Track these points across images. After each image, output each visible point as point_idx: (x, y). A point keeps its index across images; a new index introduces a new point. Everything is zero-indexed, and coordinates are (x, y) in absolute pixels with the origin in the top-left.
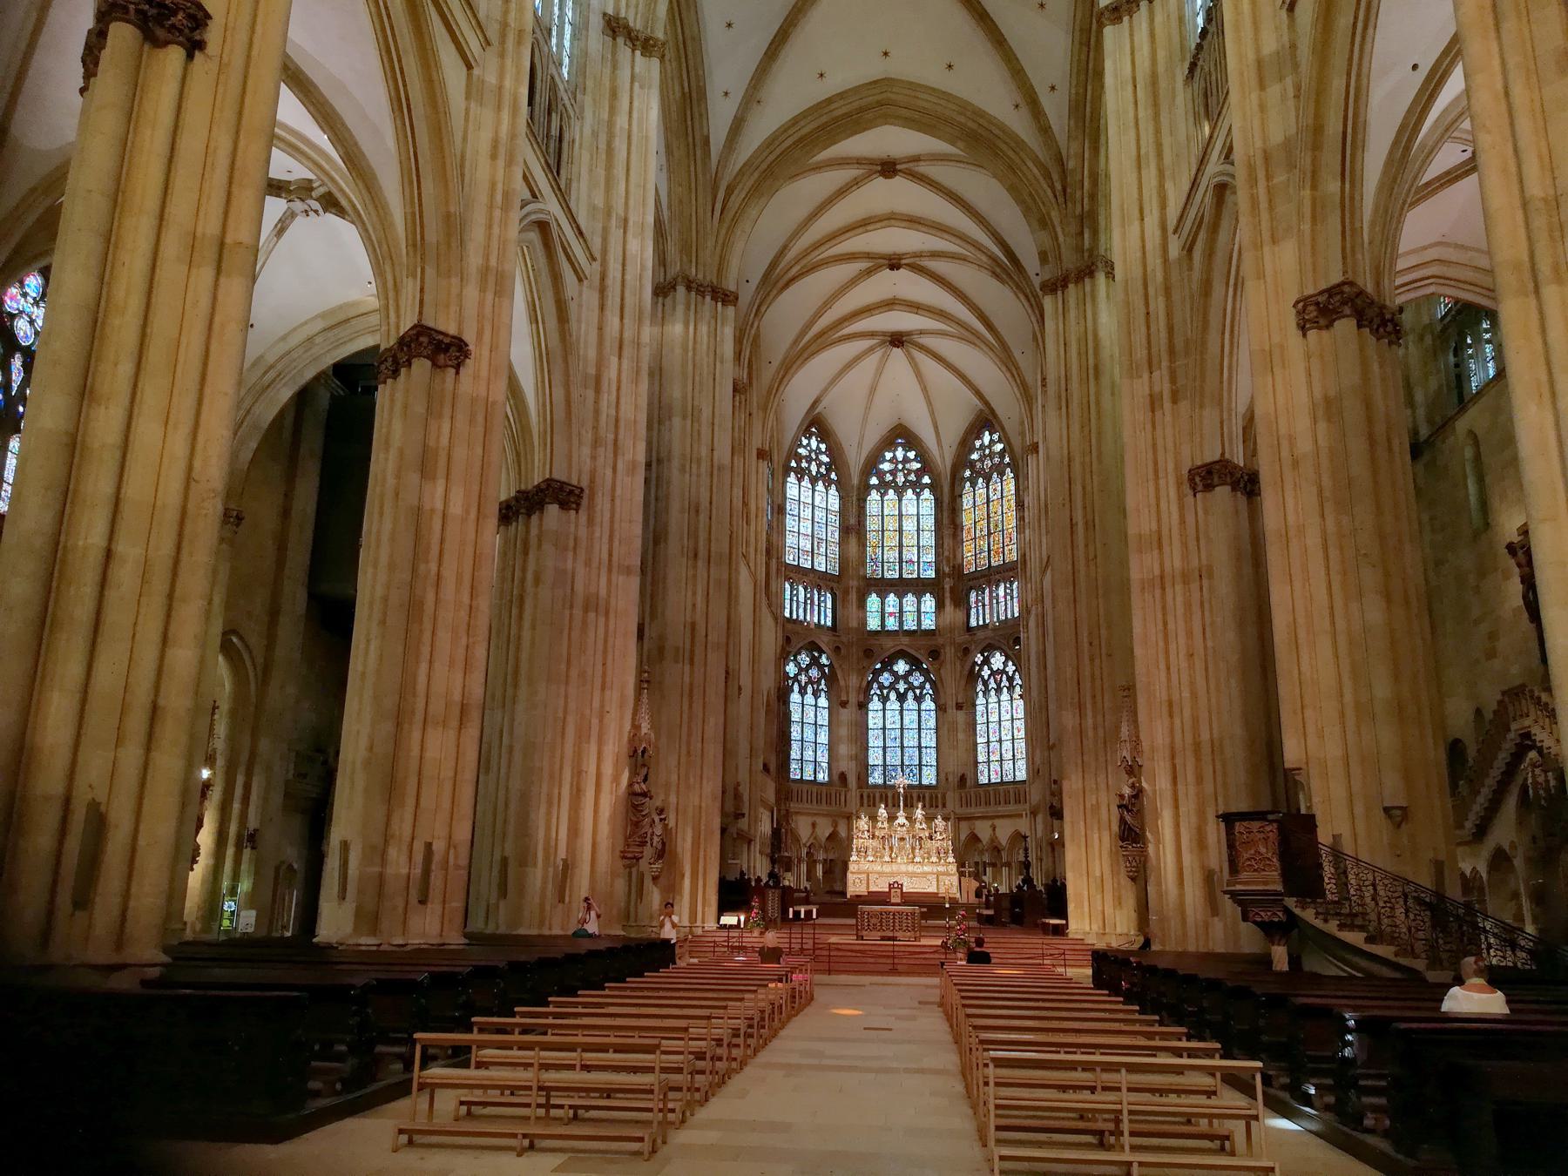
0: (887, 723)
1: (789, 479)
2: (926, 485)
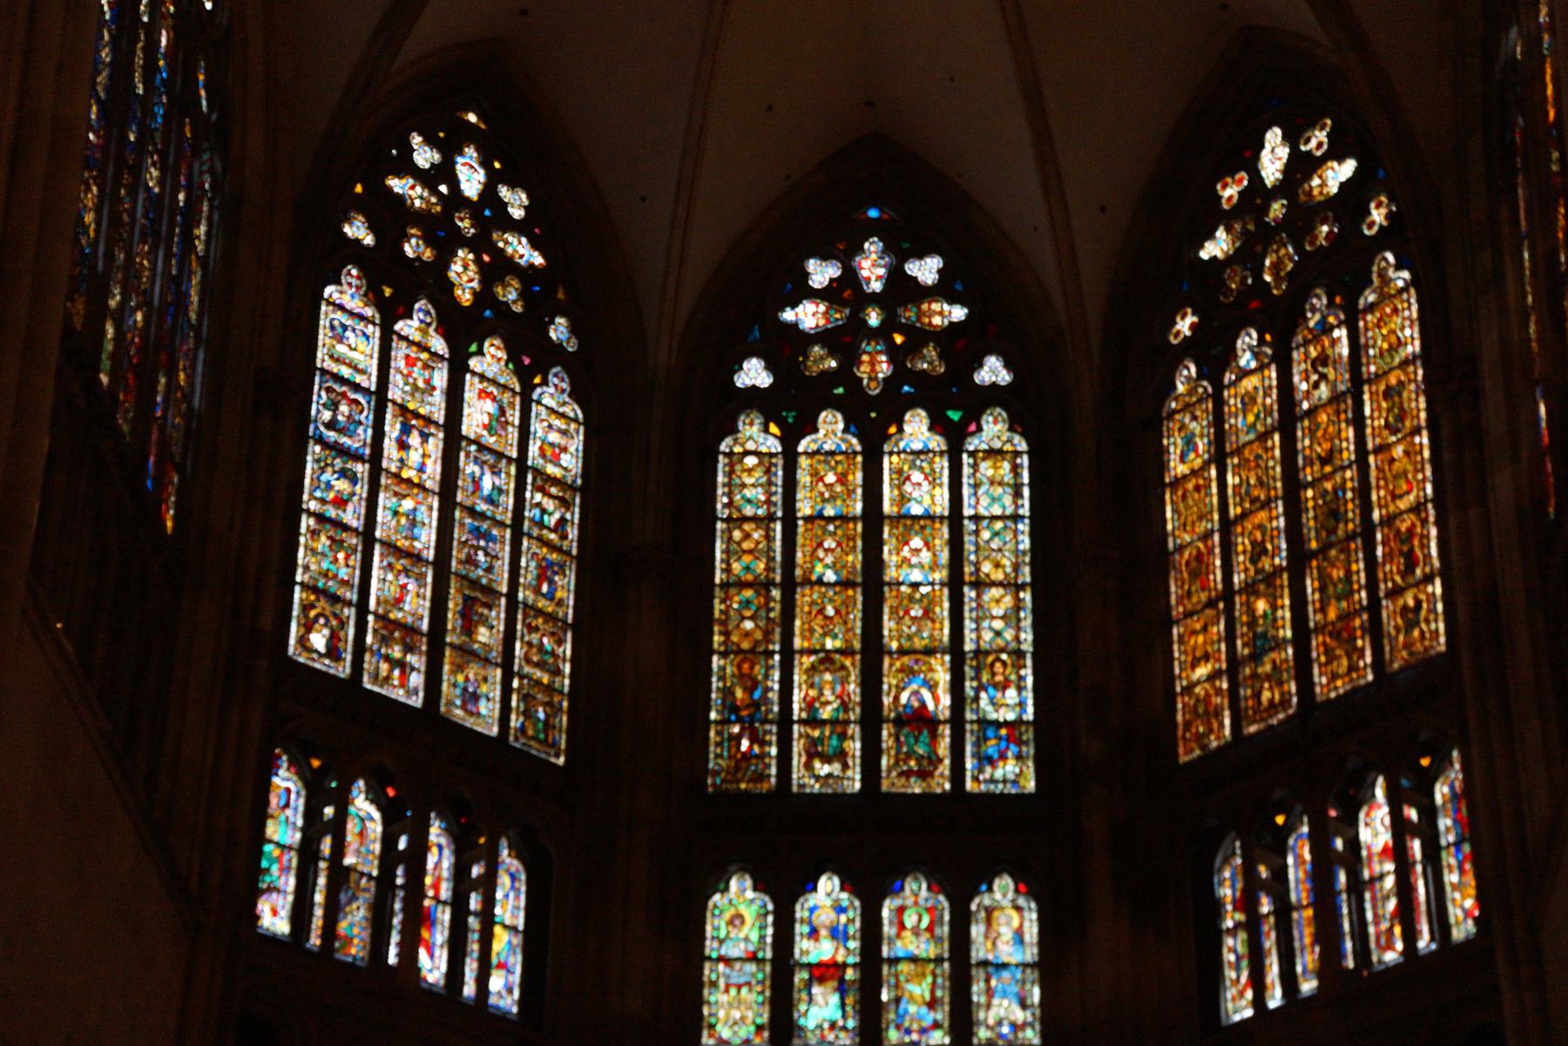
1: (329, 290)
2: (993, 396)
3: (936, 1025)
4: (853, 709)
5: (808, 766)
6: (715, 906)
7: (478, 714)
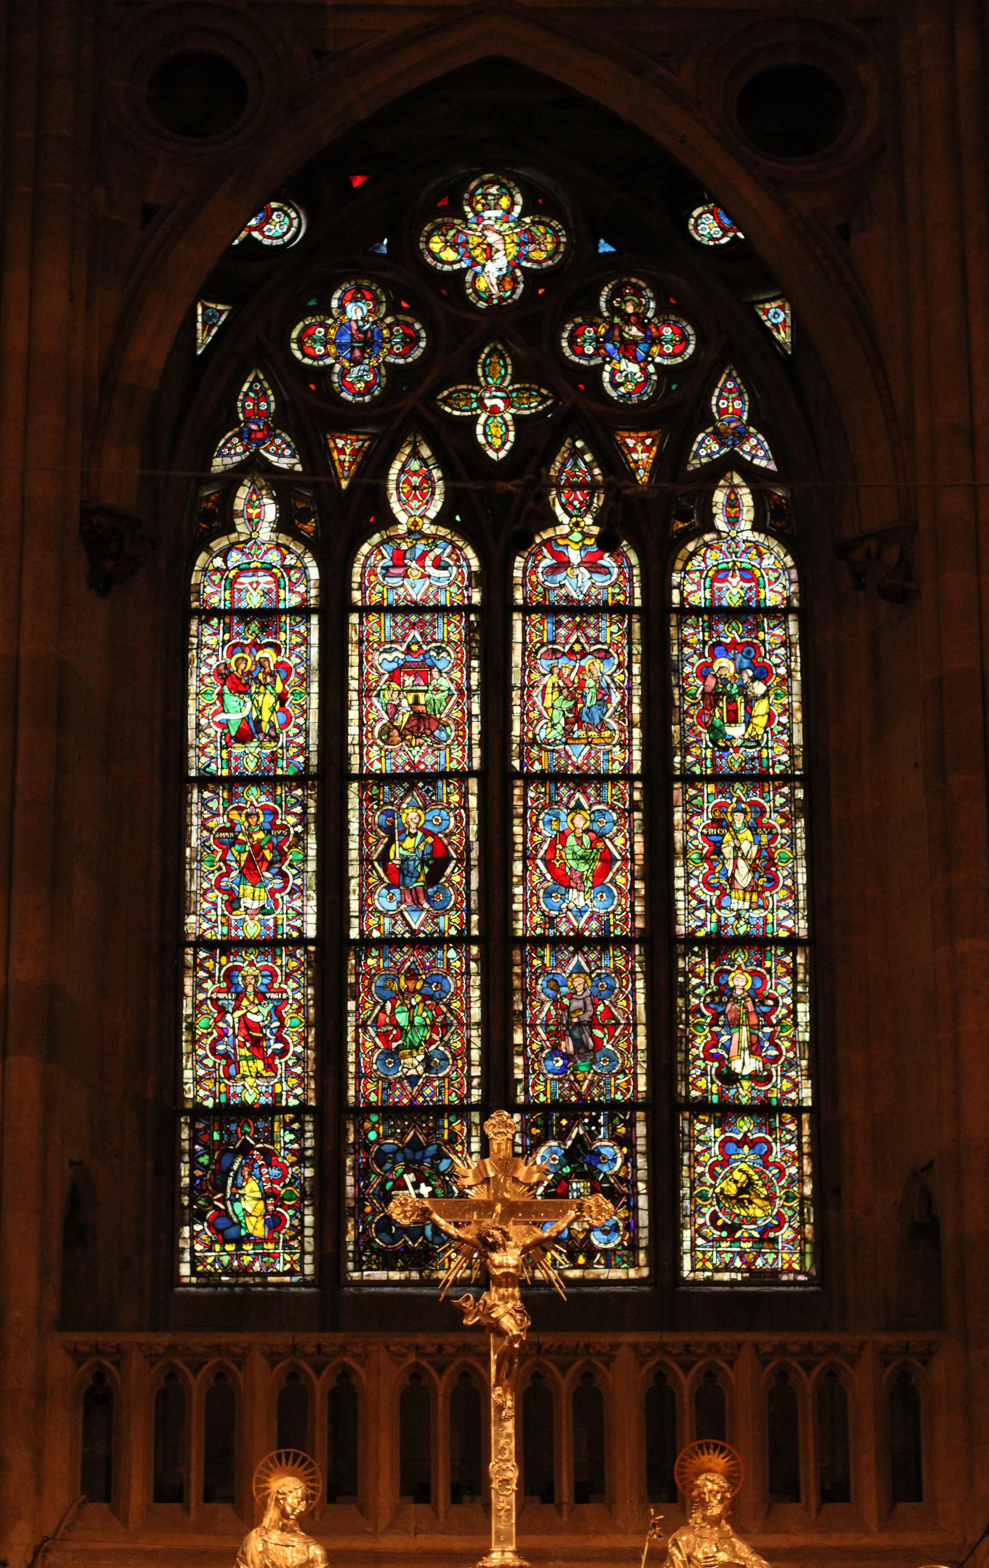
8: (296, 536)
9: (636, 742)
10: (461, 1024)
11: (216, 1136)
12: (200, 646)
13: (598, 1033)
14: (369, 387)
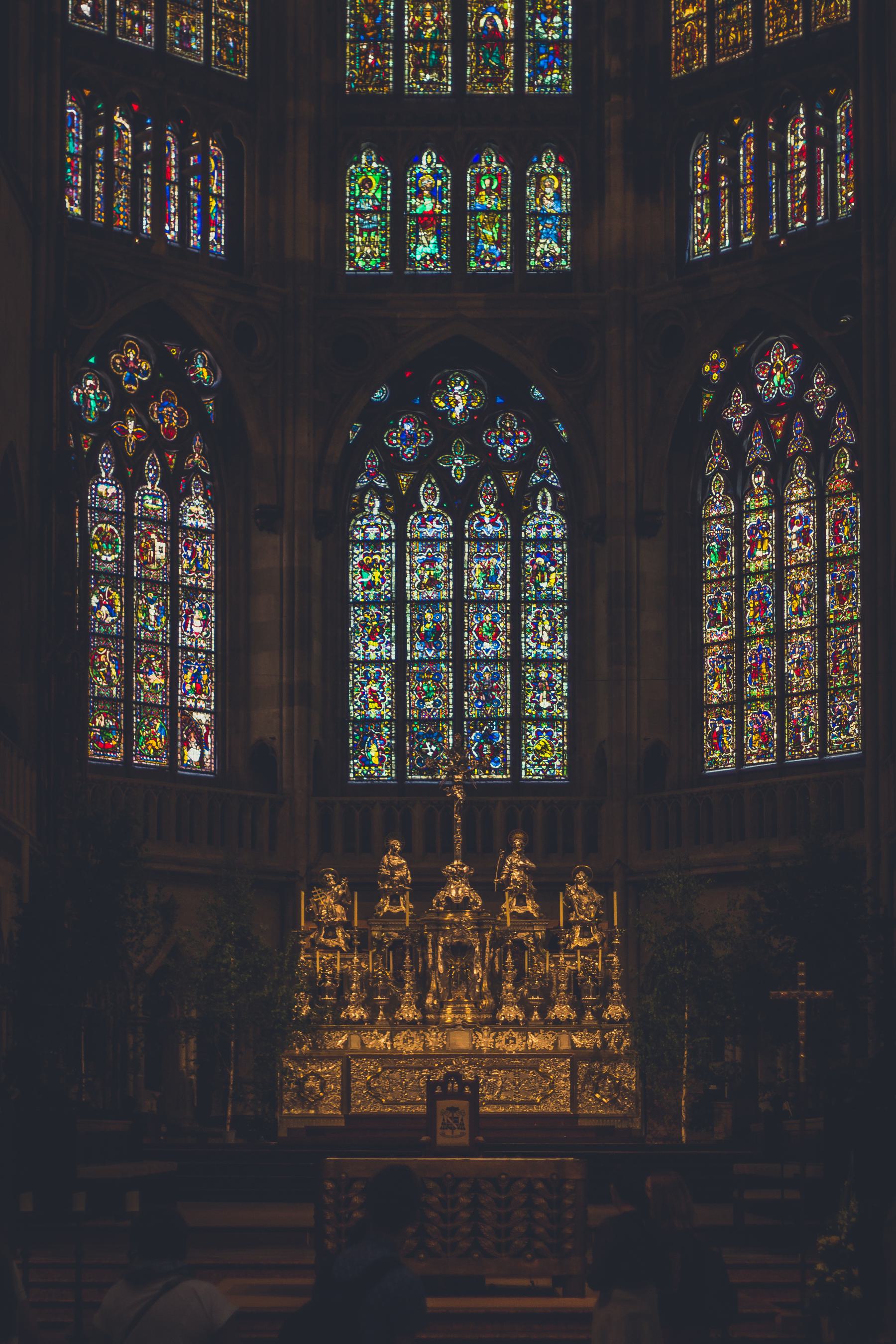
0: (412, 581)
3: (502, 258)
4: (447, 32)
5: (416, 75)
6: (352, 174)
7: (191, 49)
8: (387, 513)
9: (508, 589)
10: (446, 690)
11: (361, 729)
12: (353, 554)
13: (494, 693)
14: (412, 457)
